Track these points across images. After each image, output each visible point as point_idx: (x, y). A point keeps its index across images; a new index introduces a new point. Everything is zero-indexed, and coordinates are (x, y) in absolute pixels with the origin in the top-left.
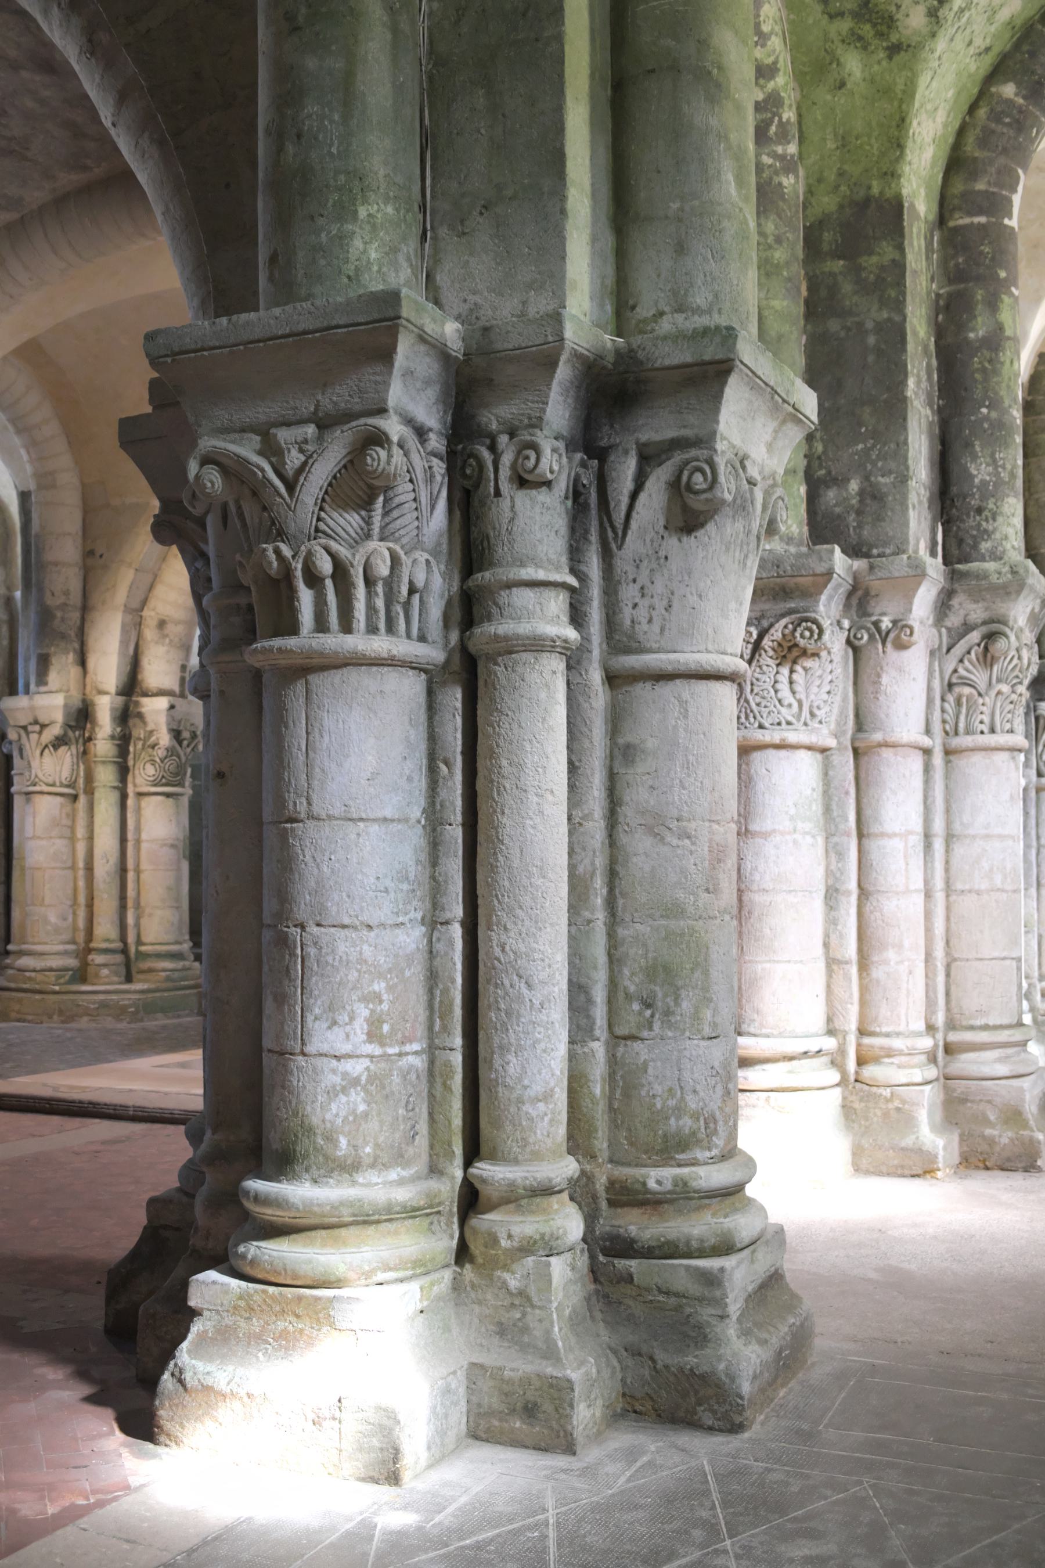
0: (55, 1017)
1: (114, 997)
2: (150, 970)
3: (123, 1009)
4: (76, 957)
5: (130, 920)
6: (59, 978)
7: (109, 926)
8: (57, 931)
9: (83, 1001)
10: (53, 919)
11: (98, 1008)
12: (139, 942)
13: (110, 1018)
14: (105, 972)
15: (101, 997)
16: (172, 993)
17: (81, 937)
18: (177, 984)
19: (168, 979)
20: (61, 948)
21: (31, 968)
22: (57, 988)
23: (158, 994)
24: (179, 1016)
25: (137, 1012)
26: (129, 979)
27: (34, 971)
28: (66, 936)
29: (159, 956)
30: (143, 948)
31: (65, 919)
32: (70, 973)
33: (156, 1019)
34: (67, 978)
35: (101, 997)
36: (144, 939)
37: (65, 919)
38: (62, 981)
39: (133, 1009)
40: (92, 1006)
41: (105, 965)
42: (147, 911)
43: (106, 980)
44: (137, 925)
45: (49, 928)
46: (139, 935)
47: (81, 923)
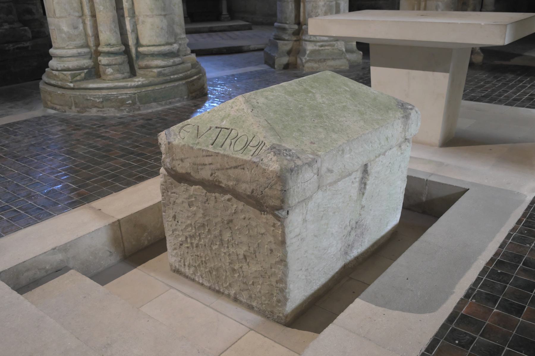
0: (73, 107)
1: (114, 93)
2: (147, 67)
3: (122, 102)
4: (90, 58)
5: (129, 27)
6: (74, 76)
7: (108, 33)
8: (70, 38)
9: (90, 96)
10: (65, 28)
11: (103, 102)
12: (138, 44)
13: (113, 109)
14: (109, 70)
15: (104, 93)
16: (163, 86)
17: (92, 43)
18: (168, 78)
19: (160, 74)
20: (75, 51)
21: (55, 68)
22: (72, 85)
23: (150, 88)
24: (170, 103)
25: (134, 103)
26: (133, 73)
27: (57, 70)
28: (80, 41)
29: (153, 55)
30: (141, 49)
31: (76, 28)
32: (86, 71)
33: (151, 108)
34: (83, 75)
35: (104, 93)
36: (143, 41)
37: (76, 28)
38: (78, 78)
39: (130, 102)
40: (98, 101)
41: (109, 65)
42: (141, 19)
43: (111, 77)
44: (135, 30)
45: (64, 35)
46: (137, 39)
47: (90, 31)
